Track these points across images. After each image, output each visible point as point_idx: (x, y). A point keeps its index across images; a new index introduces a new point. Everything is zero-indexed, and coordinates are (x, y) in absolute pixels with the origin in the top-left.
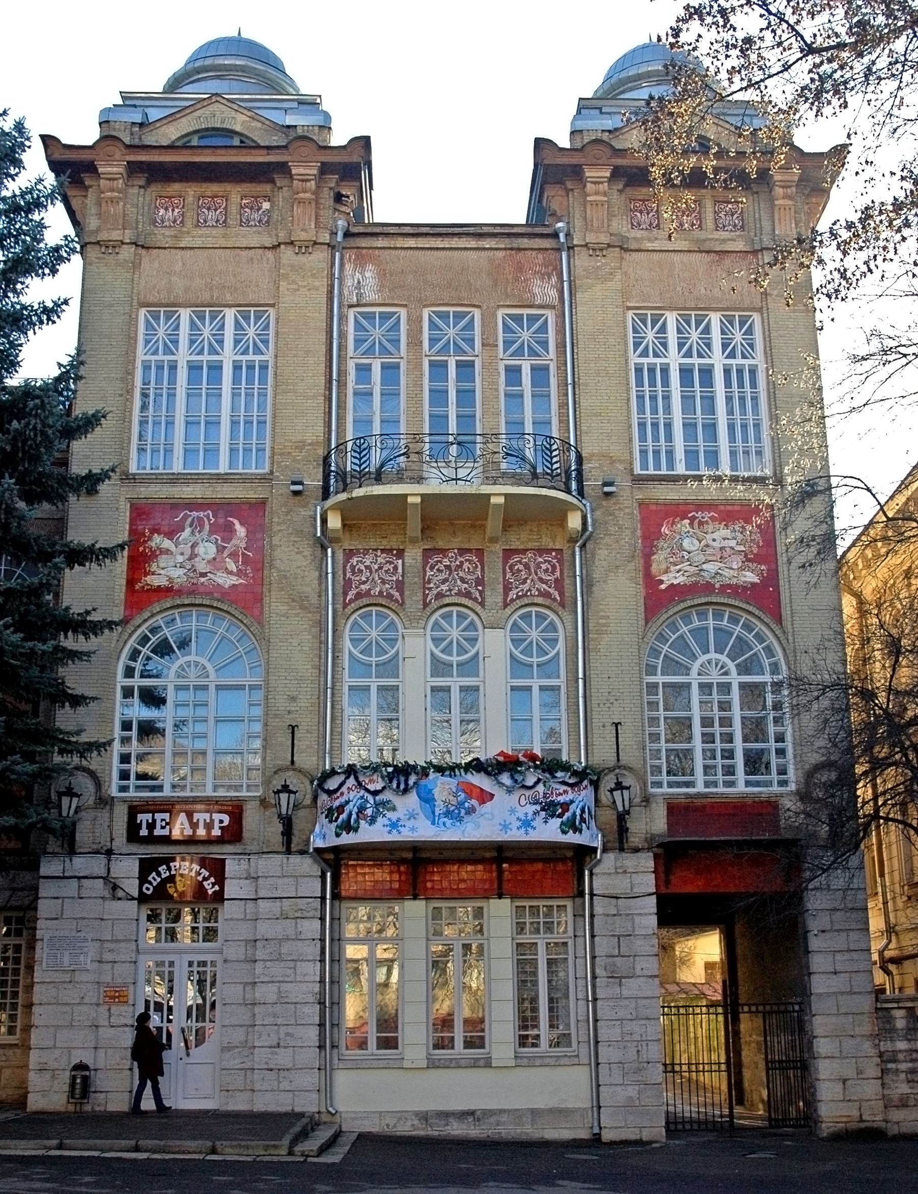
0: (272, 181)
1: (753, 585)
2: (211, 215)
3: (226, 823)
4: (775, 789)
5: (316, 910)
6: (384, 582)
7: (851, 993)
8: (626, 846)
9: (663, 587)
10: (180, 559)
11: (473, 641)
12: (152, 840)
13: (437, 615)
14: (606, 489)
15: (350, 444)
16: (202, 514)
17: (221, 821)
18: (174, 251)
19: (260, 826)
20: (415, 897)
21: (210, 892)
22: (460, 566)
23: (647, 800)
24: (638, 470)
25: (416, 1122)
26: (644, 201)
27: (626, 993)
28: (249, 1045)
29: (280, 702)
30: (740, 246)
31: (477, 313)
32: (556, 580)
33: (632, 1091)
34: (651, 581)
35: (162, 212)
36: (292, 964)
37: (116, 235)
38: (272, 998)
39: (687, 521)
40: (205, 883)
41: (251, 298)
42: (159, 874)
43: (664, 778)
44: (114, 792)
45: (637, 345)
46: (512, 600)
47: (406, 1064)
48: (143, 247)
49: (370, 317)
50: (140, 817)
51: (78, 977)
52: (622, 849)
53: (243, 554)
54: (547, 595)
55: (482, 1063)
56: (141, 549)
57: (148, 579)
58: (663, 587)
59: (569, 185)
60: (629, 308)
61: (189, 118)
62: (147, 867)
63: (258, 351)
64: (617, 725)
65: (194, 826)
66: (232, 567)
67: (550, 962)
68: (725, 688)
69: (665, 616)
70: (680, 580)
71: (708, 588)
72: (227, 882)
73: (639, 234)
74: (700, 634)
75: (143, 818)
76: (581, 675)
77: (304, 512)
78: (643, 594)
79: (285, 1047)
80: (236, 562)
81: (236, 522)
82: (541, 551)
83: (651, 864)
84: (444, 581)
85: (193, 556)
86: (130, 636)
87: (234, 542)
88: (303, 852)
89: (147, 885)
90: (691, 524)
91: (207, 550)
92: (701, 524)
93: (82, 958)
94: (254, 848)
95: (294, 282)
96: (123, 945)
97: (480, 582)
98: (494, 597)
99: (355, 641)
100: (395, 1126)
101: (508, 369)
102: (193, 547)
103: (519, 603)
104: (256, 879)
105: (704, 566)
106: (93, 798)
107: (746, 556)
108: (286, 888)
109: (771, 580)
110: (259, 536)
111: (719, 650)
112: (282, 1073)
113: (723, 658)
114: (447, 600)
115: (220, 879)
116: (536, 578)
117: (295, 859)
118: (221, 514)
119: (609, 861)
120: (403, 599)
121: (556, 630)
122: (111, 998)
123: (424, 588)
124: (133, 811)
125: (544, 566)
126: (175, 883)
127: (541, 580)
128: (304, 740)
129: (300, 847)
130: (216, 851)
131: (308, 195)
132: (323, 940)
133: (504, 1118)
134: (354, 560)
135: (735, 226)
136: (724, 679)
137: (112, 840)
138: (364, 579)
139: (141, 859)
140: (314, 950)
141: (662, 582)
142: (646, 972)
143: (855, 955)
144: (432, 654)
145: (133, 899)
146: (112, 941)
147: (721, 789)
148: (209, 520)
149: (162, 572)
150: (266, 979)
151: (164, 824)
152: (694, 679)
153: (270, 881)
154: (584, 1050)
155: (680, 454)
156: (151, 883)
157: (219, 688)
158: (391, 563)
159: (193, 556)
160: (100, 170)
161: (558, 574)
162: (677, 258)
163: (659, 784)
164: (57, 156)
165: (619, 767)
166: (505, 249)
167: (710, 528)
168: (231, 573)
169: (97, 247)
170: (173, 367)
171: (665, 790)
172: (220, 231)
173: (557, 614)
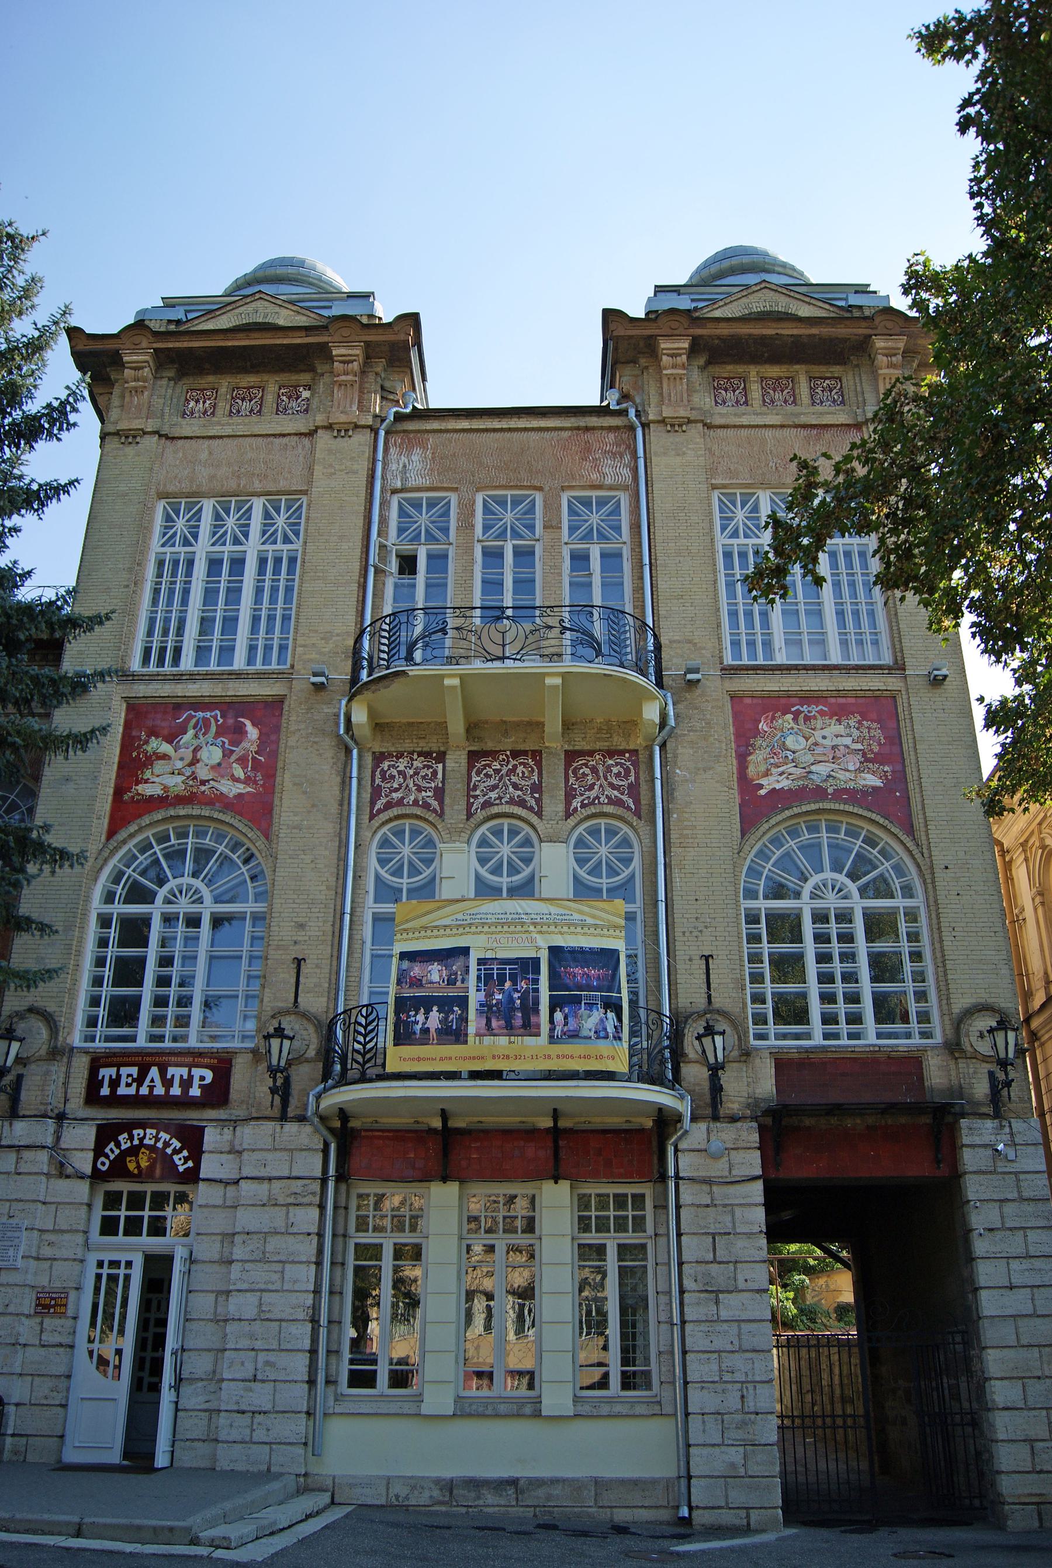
0: (312, 369)
1: (875, 789)
2: (245, 406)
3: (209, 1079)
4: (916, 1041)
5: (314, 1194)
7: (1035, 1315)
8: (722, 1113)
9: (762, 792)
10: (179, 765)
12: (115, 1101)
13: (483, 829)
16: (208, 714)
17: (202, 1078)
18: (201, 441)
19: (248, 1083)
20: (445, 1179)
21: (181, 1169)
22: (514, 770)
23: (746, 1054)
24: (729, 660)
25: (436, 1493)
26: (729, 379)
27: (724, 1314)
28: (218, 1376)
29: (282, 930)
30: (842, 419)
31: (539, 497)
32: (630, 785)
33: (735, 1455)
34: (746, 785)
35: (192, 404)
36: (278, 1267)
37: (136, 424)
38: (250, 1312)
39: (789, 717)
40: (176, 1158)
41: (282, 485)
42: (118, 1145)
43: (771, 1028)
45: (723, 528)
46: (576, 809)
47: (425, 1409)
48: (167, 437)
49: (417, 505)
52: (716, 1118)
53: (254, 758)
54: (619, 803)
55: (528, 1410)
56: (134, 754)
57: (140, 788)
58: (762, 792)
59: (643, 361)
60: (714, 487)
62: (106, 1134)
63: (287, 540)
64: (707, 958)
65: (168, 1083)
66: (239, 772)
67: (623, 1272)
68: (844, 917)
69: (766, 826)
70: (784, 783)
71: (820, 793)
72: (205, 1157)
73: (721, 409)
74: (812, 850)
76: (662, 896)
77: (328, 710)
78: (738, 801)
79: (263, 1381)
81: (248, 723)
82: (611, 753)
83: (755, 1137)
84: (494, 788)
85: (195, 761)
87: (244, 744)
88: (302, 1119)
89: (102, 1159)
90: (795, 719)
91: (212, 754)
92: (807, 719)
93: (11, 1252)
95: (331, 466)
96: (67, 1237)
97: (537, 788)
98: (554, 805)
99: (382, 862)
100: (407, 1498)
102: (196, 750)
104: (240, 1153)
105: (813, 768)
106: (45, 1047)
107: (864, 755)
108: (278, 1165)
109: (898, 780)
110: (273, 737)
111: (837, 868)
112: (259, 1418)
113: (842, 878)
114: (495, 810)
116: (604, 784)
117: (291, 1128)
118: (231, 714)
119: (696, 1134)
120: (442, 809)
122: (45, 1307)
123: (468, 796)
124: (97, 1062)
125: (615, 770)
126: (137, 1156)
127: (613, 786)
128: (314, 976)
129: (299, 1112)
130: (192, 1116)
132: (320, 1235)
133: (556, 1491)
134: (385, 765)
135: (834, 401)
137: (66, 1100)
138: (396, 785)
139: (100, 1127)
140: (308, 1248)
141: (761, 787)
143: (1038, 1263)
144: (478, 878)
145: (82, 1177)
146: (54, 1231)
147: (844, 1041)
148: (217, 721)
149: (156, 779)
150: (245, 1286)
151: (130, 1080)
153: (257, 1155)
156: (107, 1157)
158: (429, 767)
159: (195, 761)
160: (126, 359)
161: (632, 778)
162: (768, 433)
164: (80, 347)
165: (710, 1012)
167: (819, 723)
168: (237, 780)
169: (116, 439)
171: (772, 1042)
172: (254, 418)
173: (631, 826)
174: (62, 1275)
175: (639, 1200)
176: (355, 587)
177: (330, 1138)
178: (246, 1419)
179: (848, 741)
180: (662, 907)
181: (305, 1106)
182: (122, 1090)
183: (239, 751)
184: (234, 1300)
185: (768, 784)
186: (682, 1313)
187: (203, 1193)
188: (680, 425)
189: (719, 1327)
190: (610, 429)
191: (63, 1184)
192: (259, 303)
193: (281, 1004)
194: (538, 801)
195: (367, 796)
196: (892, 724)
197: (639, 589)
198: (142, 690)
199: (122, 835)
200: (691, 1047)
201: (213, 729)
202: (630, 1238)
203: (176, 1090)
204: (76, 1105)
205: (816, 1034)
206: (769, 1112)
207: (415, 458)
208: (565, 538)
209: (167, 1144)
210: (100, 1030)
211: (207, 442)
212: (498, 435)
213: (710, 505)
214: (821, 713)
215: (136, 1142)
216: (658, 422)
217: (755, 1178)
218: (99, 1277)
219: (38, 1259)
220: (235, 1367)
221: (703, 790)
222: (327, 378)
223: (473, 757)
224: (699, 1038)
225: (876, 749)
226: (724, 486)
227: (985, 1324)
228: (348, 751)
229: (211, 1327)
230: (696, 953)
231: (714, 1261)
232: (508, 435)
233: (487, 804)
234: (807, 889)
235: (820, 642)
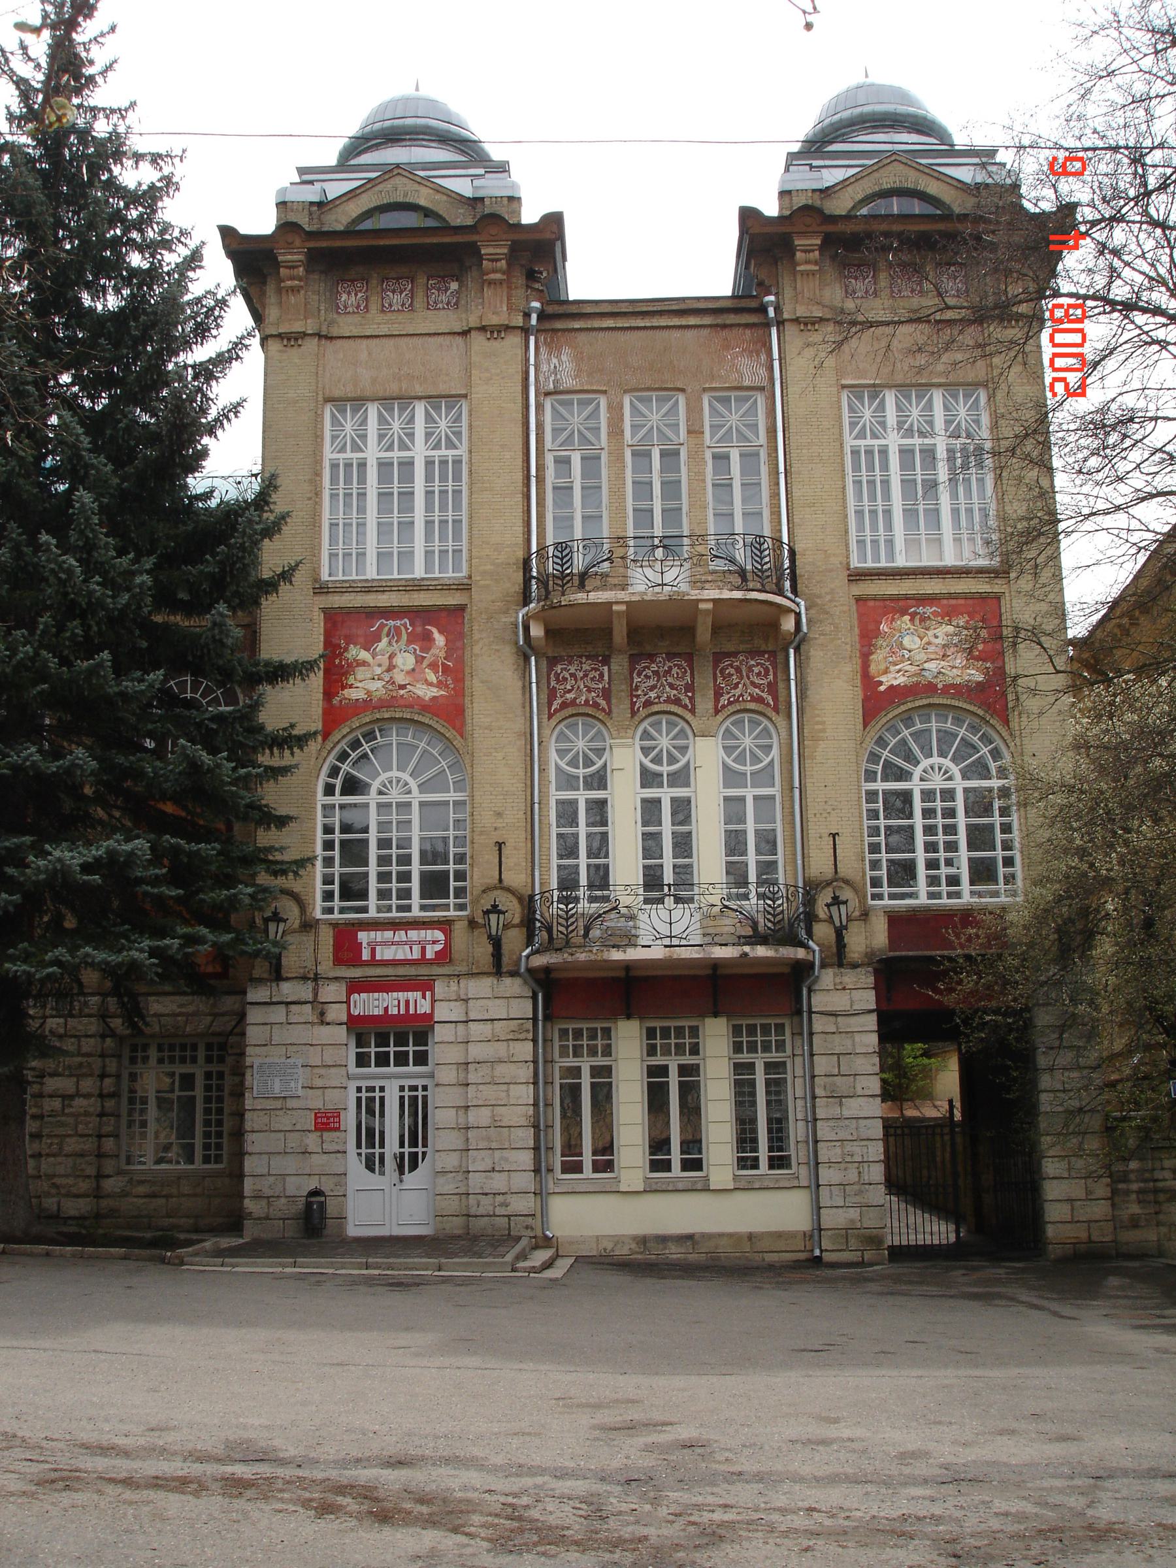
1: (978, 683)
2: (396, 299)
4: (1003, 899)
9: (882, 688)
10: (378, 671)
11: (683, 749)
13: (645, 724)
15: (551, 549)
16: (398, 623)
24: (855, 563)
25: (633, 1246)
27: (846, 1113)
32: (769, 684)
33: (853, 1214)
34: (868, 681)
35: (344, 297)
36: (504, 1087)
41: (442, 389)
43: (885, 890)
44: (318, 914)
46: (724, 707)
52: (840, 965)
54: (759, 700)
57: (346, 692)
58: (882, 688)
61: (369, 193)
63: (451, 445)
64: (834, 835)
66: (432, 677)
68: (948, 794)
69: (884, 720)
70: (900, 680)
71: (931, 688)
78: (861, 697)
80: (436, 672)
81: (435, 630)
83: (871, 979)
85: (391, 668)
86: (329, 752)
87: (433, 651)
88: (514, 974)
90: (912, 620)
91: (406, 661)
92: (923, 619)
94: (462, 969)
96: (333, 1070)
97: (690, 688)
98: (705, 704)
99: (561, 753)
102: (391, 657)
103: (732, 709)
104: (466, 1001)
105: (926, 666)
108: (498, 1009)
110: (459, 644)
111: (942, 754)
114: (656, 708)
119: (827, 978)
123: (632, 696)
125: (756, 670)
128: (515, 858)
131: (498, 276)
132: (535, 1062)
134: (558, 668)
136: (948, 785)
140: (526, 1073)
141: (881, 683)
144: (641, 764)
147: (945, 901)
152: (915, 786)
154: (803, 1172)
157: (422, 804)
158: (596, 670)
159: (391, 668)
163: (879, 897)
166: (710, 326)
168: (431, 684)
169: (278, 340)
170: (362, 465)
171: (886, 902)
174: (332, 1099)
175: (780, 1028)
176: (519, 498)
177: (537, 988)
180: (797, 792)
183: (429, 657)
184: (472, 1113)
186: (814, 1113)
189: (841, 1123)
190: (747, 326)
192: (398, 181)
194: (691, 699)
195: (544, 697)
197: (775, 495)
198: (337, 601)
199: (336, 736)
200: (822, 912)
201: (404, 636)
202: (774, 1056)
204: (326, 966)
205: (922, 896)
206: (880, 961)
207: (564, 358)
208: (708, 443)
210: (337, 903)
211: (365, 342)
213: (840, 408)
216: (792, 320)
218: (359, 1099)
221: (834, 694)
222: (475, 273)
223: (634, 659)
224: (828, 905)
228: (527, 659)
229: (455, 1133)
230: (825, 832)
231: (839, 1075)
232: (650, 333)
233: (648, 703)
234: (917, 772)
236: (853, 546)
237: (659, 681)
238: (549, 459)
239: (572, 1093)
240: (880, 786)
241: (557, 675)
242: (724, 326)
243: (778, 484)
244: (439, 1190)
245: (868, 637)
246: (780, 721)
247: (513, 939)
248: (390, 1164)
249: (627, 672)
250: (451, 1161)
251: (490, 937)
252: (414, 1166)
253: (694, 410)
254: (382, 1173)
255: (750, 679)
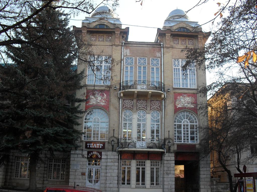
0: (112, 34)
1: (193, 107)
4: (195, 143)
6: (130, 105)
11: (145, 116)
14: (168, 90)
17: (101, 145)
22: (143, 103)
23: (174, 144)
24: (174, 87)
27: (169, 177)
34: (175, 106)
36: (113, 170)
38: (110, 175)
39: (182, 96)
42: (91, 154)
44: (83, 140)
50: (88, 144)
51: (77, 171)
52: (169, 153)
57: (89, 103)
58: (178, 107)
60: (173, 58)
62: (89, 153)
64: (169, 131)
65: (97, 146)
66: (104, 101)
67: (156, 171)
68: (187, 125)
70: (180, 106)
71: (185, 108)
74: (184, 116)
75: (88, 144)
76: (163, 122)
77: (116, 93)
81: (104, 94)
87: (104, 97)
88: (115, 151)
90: (183, 97)
91: (99, 98)
92: (184, 97)
94: (107, 150)
95: (115, 52)
96: (84, 166)
97: (146, 106)
98: (149, 109)
99: (125, 115)
101: (152, 68)
104: (107, 155)
105: (185, 104)
108: (112, 157)
111: (187, 119)
113: (187, 120)
114: (141, 109)
115: (101, 156)
117: (114, 152)
119: (167, 154)
121: (159, 114)
125: (157, 103)
129: (115, 150)
130: (100, 151)
131: (118, 37)
132: (118, 166)
134: (125, 101)
136: (187, 124)
140: (117, 168)
142: (172, 173)
144: (138, 118)
147: (186, 143)
154: (161, 186)
155: (181, 84)
160: (82, 32)
163: (176, 142)
167: (186, 97)
168: (103, 103)
171: (177, 142)
173: (159, 111)
174: (84, 171)
178: (110, 188)
179: (190, 100)
181: (116, 149)
182: (91, 147)
183: (103, 98)
185: (179, 106)
186: (164, 176)
187: (103, 160)
188: (168, 48)
191: (83, 159)
193: (111, 136)
196: (196, 98)
197: (161, 75)
200: (166, 143)
202: (157, 167)
203: (98, 147)
204: (84, 148)
208: (151, 66)
209: (97, 154)
212: (140, 47)
214: (186, 96)
215: (93, 154)
217: (174, 160)
219: (81, 168)
220: (108, 182)
223: (137, 100)
225: (193, 102)
226: (174, 58)
227: (200, 179)
228: (120, 99)
231: (168, 170)
232: (142, 47)
234: (183, 121)
235: (187, 84)
236: (174, 84)
237: (141, 104)
238: (125, 66)
239: (124, 171)
240: (176, 123)
241: (124, 102)
242: (154, 47)
243: (162, 73)
244: (101, 186)
245: (176, 99)
246: (161, 112)
247: (116, 145)
248: (93, 182)
249: (136, 102)
250: (103, 182)
251: (112, 145)
252: (97, 182)
253: (149, 60)
254: (92, 183)
255: (156, 104)
